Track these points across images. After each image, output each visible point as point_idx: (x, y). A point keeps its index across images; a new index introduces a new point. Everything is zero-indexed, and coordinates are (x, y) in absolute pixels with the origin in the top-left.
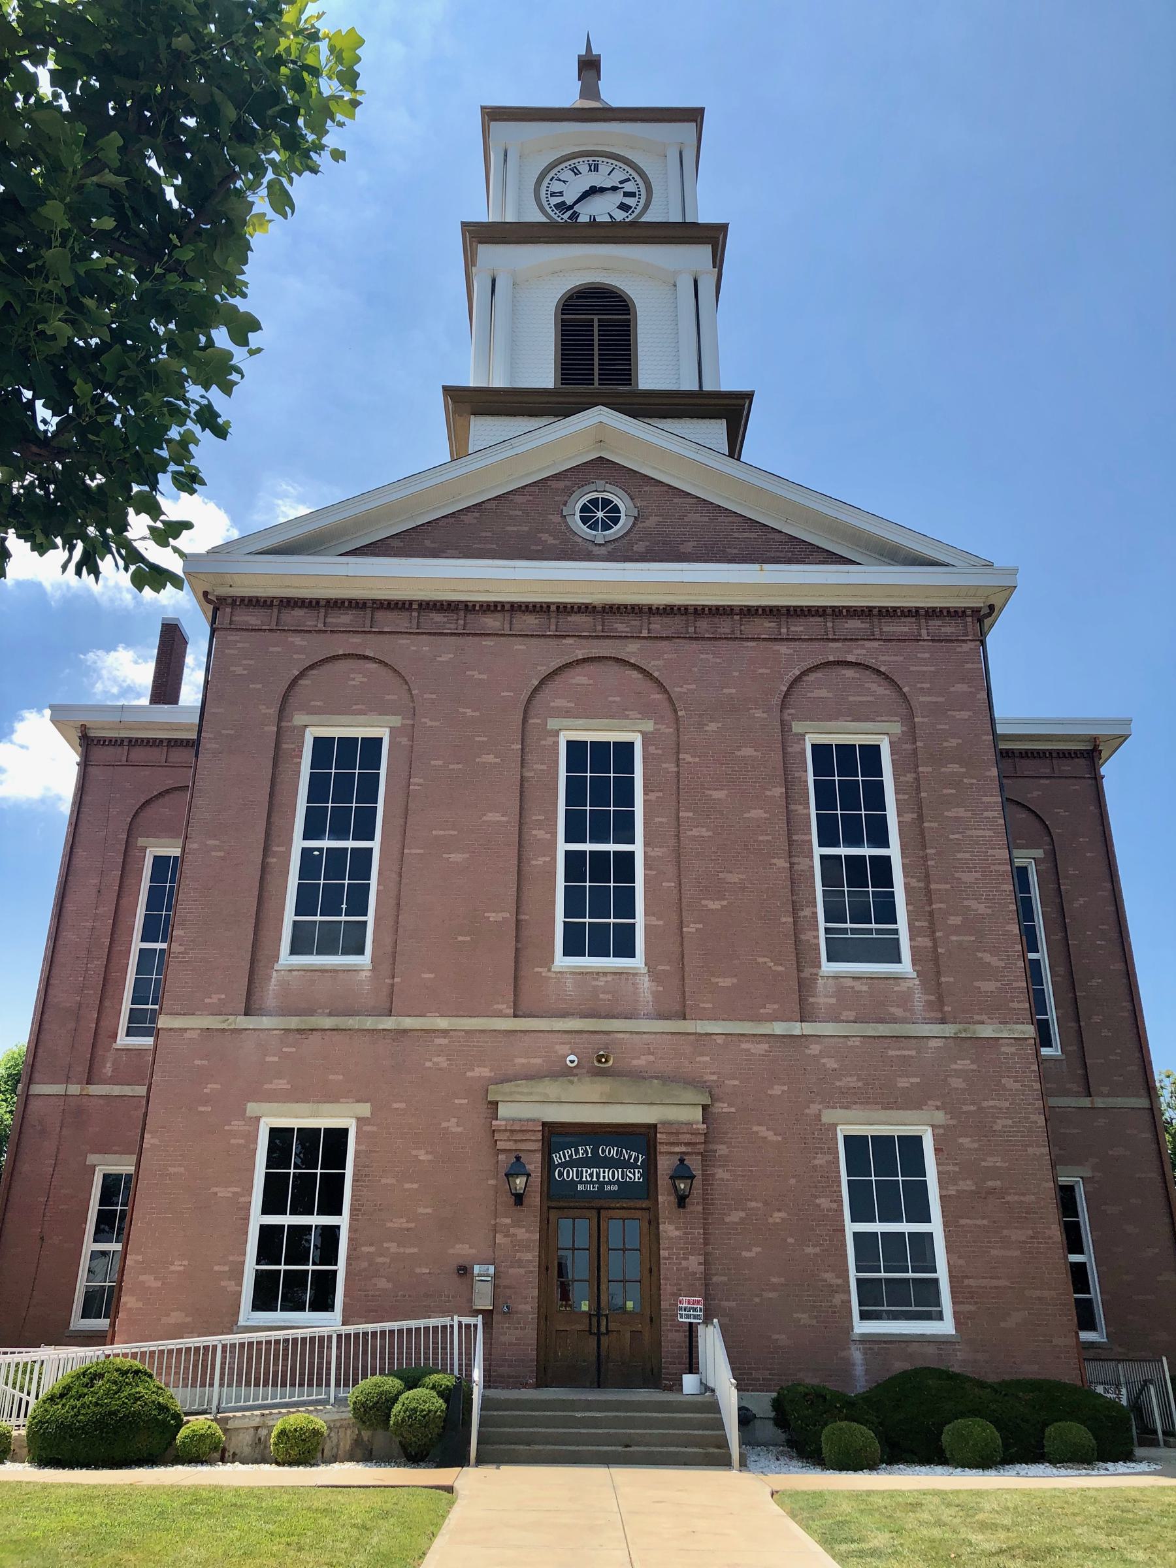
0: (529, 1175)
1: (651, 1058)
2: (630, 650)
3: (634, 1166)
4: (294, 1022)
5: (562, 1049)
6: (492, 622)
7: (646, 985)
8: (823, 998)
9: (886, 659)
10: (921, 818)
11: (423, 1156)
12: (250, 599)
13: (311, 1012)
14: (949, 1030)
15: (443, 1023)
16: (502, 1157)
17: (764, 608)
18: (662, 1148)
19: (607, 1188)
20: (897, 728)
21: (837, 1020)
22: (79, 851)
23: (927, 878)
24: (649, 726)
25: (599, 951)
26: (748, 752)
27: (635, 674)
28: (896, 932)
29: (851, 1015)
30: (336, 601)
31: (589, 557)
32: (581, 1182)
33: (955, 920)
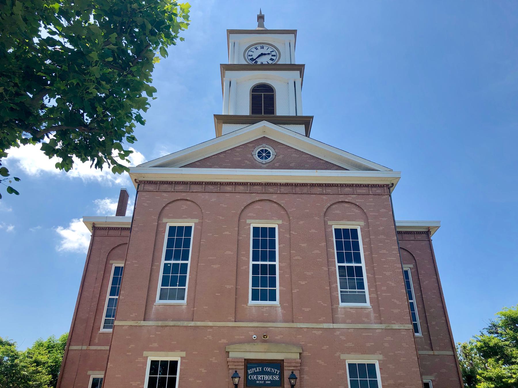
0: (240, 378)
1: (282, 336)
2: (274, 197)
3: (276, 374)
4: (160, 323)
5: (251, 333)
6: (229, 188)
7: (280, 310)
8: (340, 315)
10: (371, 253)
11: (204, 371)
12: (150, 182)
13: (166, 320)
14: (383, 326)
15: (210, 324)
16: (231, 371)
17: (318, 184)
18: (285, 368)
19: (267, 382)
20: (362, 223)
21: (344, 322)
22: (90, 265)
23: (374, 274)
24: (280, 222)
25: (264, 299)
26: (313, 231)
27: (275, 205)
28: (364, 292)
29: (350, 321)
30: (178, 182)
31: (261, 168)
32: (258, 380)
33: (384, 288)
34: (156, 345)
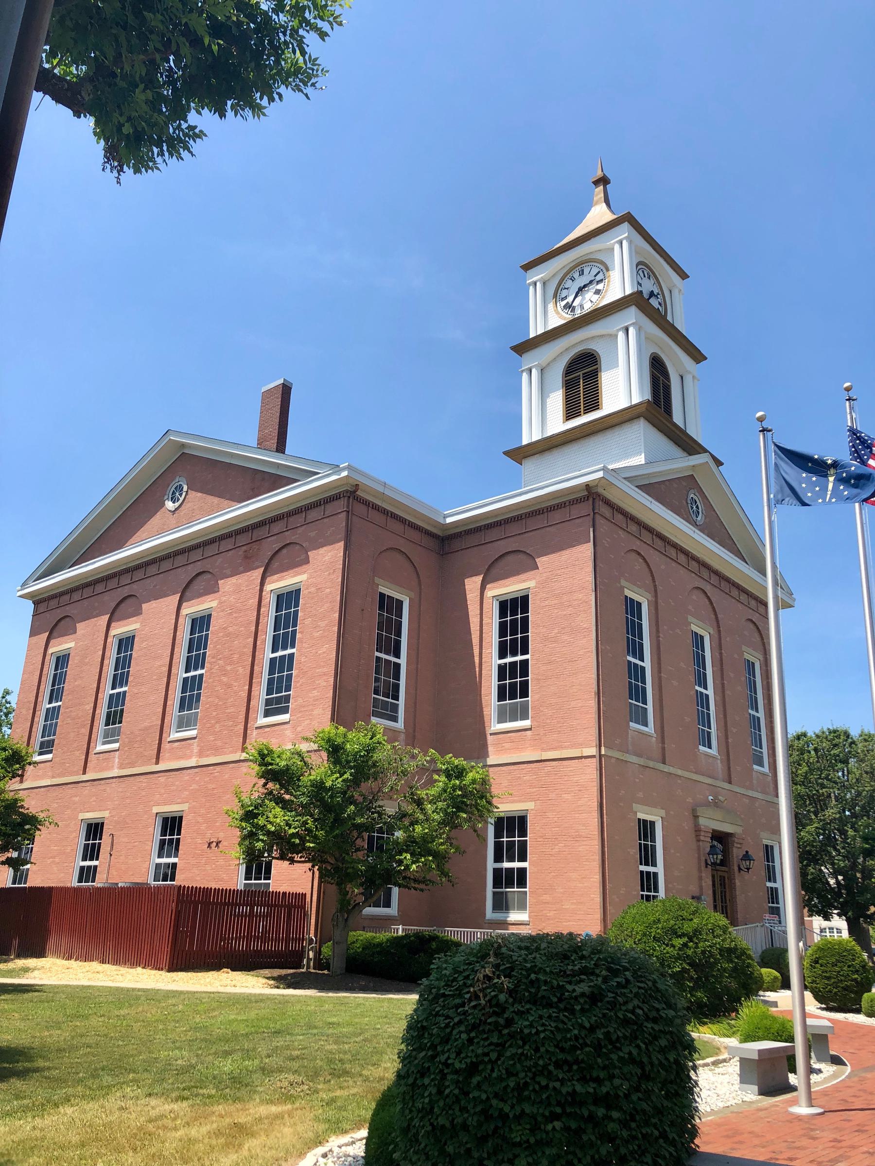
7: (720, 765)
15: (680, 772)
20: (761, 657)
28: (761, 753)
34: (640, 795)
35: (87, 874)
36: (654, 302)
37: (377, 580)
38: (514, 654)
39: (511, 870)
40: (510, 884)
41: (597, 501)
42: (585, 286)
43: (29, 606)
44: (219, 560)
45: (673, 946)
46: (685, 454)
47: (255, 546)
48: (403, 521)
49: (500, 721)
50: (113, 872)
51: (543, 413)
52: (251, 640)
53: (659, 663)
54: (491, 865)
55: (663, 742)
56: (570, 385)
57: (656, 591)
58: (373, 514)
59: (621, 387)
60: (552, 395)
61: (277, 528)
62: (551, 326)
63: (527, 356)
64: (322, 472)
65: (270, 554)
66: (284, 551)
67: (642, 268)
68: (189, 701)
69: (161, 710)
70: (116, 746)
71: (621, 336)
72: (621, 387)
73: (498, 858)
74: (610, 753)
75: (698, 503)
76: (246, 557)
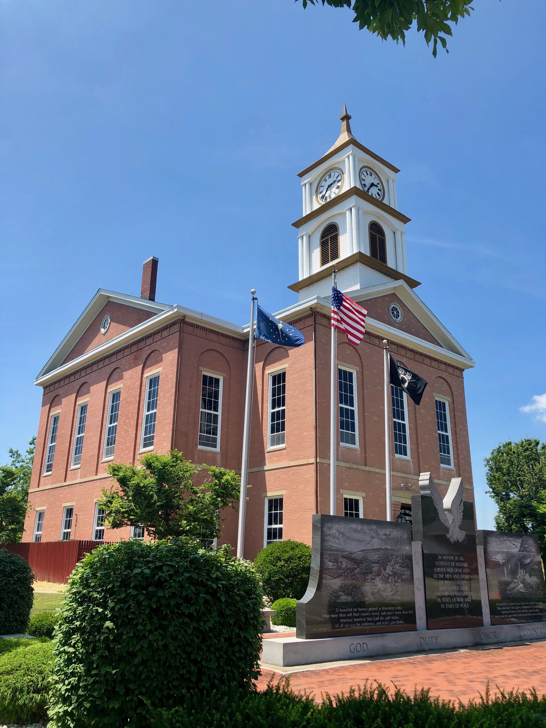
4: (347, 465)
7: (412, 465)
9: (449, 379)
10: (455, 426)
20: (450, 400)
28: (449, 457)
29: (445, 479)
35: (67, 535)
36: (374, 191)
37: (201, 368)
38: (279, 406)
39: (275, 529)
40: (275, 537)
41: (317, 317)
42: (331, 184)
43: (41, 389)
44: (124, 360)
45: (276, 566)
46: (393, 280)
47: (139, 352)
48: (217, 333)
49: (272, 445)
50: (77, 535)
51: (310, 263)
52: (137, 405)
53: (364, 408)
54: (266, 526)
55: (366, 453)
56: (324, 244)
57: (362, 365)
58: (198, 331)
59: (349, 244)
60: (315, 251)
61: (149, 341)
62: (314, 209)
63: (301, 228)
64: (166, 309)
65: (146, 356)
66: (152, 355)
67: (363, 170)
68: (111, 442)
69: (98, 445)
70: (79, 466)
71: (348, 213)
72: (349, 244)
73: (270, 523)
74: (323, 461)
75: (398, 309)
76: (136, 359)
